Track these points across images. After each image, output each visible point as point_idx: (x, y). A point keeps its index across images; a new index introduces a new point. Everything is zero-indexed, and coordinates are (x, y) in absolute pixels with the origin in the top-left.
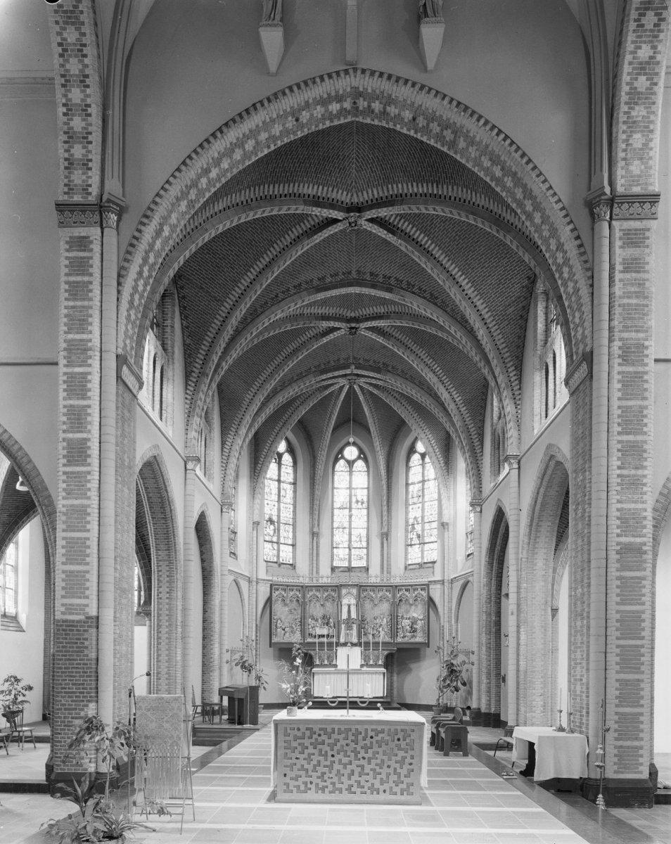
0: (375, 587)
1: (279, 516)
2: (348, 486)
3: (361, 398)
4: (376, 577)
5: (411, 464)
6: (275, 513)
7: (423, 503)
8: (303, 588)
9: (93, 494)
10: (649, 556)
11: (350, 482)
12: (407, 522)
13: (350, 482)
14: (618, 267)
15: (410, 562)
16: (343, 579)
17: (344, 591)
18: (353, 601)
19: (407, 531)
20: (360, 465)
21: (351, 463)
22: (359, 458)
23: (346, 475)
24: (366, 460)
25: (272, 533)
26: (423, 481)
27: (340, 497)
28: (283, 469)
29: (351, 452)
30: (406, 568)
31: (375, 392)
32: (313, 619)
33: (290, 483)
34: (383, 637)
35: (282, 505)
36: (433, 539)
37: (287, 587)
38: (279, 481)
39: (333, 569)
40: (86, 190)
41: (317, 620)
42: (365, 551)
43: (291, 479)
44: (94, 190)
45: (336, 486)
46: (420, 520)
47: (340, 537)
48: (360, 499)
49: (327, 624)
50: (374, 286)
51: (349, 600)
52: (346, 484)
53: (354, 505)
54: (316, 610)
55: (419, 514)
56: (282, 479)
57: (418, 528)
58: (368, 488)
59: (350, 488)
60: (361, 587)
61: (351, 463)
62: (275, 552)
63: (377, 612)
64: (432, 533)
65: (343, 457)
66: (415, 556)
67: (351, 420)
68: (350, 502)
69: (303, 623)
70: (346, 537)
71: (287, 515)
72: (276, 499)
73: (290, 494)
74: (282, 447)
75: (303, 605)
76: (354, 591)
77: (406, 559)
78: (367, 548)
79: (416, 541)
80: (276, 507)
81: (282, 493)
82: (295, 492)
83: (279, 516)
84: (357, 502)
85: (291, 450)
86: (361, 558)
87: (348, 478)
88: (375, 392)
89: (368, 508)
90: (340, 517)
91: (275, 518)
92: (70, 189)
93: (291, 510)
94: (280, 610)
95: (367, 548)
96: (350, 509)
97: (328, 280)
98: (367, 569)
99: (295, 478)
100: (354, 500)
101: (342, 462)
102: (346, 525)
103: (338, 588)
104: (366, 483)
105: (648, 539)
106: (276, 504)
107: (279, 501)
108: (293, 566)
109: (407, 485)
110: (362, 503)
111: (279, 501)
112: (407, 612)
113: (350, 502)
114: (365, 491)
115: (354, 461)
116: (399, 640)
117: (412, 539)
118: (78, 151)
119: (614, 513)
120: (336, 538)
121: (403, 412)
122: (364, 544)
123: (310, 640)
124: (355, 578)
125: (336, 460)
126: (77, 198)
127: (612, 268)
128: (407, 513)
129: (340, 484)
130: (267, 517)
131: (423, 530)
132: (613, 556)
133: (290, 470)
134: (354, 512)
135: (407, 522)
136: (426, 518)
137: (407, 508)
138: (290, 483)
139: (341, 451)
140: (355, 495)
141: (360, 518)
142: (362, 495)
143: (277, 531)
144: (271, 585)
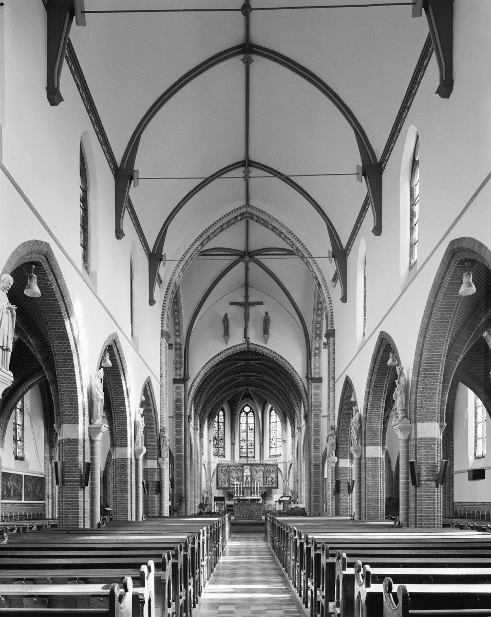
0: (257, 465)
1: (218, 436)
3: (251, 393)
4: (258, 461)
5: (271, 414)
7: (276, 431)
8: (228, 466)
9: (183, 452)
10: (321, 466)
11: (247, 421)
12: (270, 438)
13: (247, 421)
14: (313, 395)
15: (271, 455)
16: (244, 461)
17: (245, 467)
18: (249, 471)
19: (270, 442)
20: (251, 414)
21: (247, 413)
22: (250, 411)
23: (245, 418)
24: (253, 412)
26: (276, 422)
27: (243, 427)
29: (247, 409)
30: (270, 457)
31: (257, 392)
32: (233, 478)
34: (260, 484)
37: (223, 466)
38: (218, 422)
39: (240, 457)
40: (180, 375)
41: (234, 479)
44: (182, 375)
46: (275, 437)
49: (238, 480)
50: (254, 372)
51: (247, 472)
52: (245, 422)
54: (234, 475)
55: (275, 435)
57: (274, 440)
58: (254, 424)
59: (247, 424)
60: (251, 465)
61: (247, 413)
63: (258, 475)
64: (279, 443)
65: (244, 411)
66: (273, 452)
67: (247, 396)
68: (247, 429)
69: (229, 480)
70: (245, 444)
75: (228, 472)
76: (249, 467)
77: (270, 453)
78: (254, 448)
79: (274, 446)
81: (219, 427)
82: (224, 426)
83: (218, 436)
84: (250, 429)
87: (246, 419)
88: (257, 392)
89: (254, 432)
91: (217, 437)
92: (176, 375)
94: (221, 476)
96: (247, 432)
97: (239, 371)
98: (254, 457)
99: (224, 421)
100: (248, 428)
101: (243, 413)
102: (245, 439)
103: (242, 465)
105: (321, 462)
108: (224, 456)
110: (252, 430)
112: (270, 475)
113: (247, 429)
116: (267, 486)
118: (178, 366)
119: (312, 456)
120: (242, 444)
121: (267, 399)
122: (253, 447)
123: (231, 486)
124: (251, 461)
125: (241, 412)
126: (178, 377)
127: (311, 394)
128: (270, 435)
131: (276, 442)
132: (312, 466)
133: (222, 417)
135: (270, 438)
137: (270, 432)
139: (243, 408)
142: (252, 426)
144: (217, 465)
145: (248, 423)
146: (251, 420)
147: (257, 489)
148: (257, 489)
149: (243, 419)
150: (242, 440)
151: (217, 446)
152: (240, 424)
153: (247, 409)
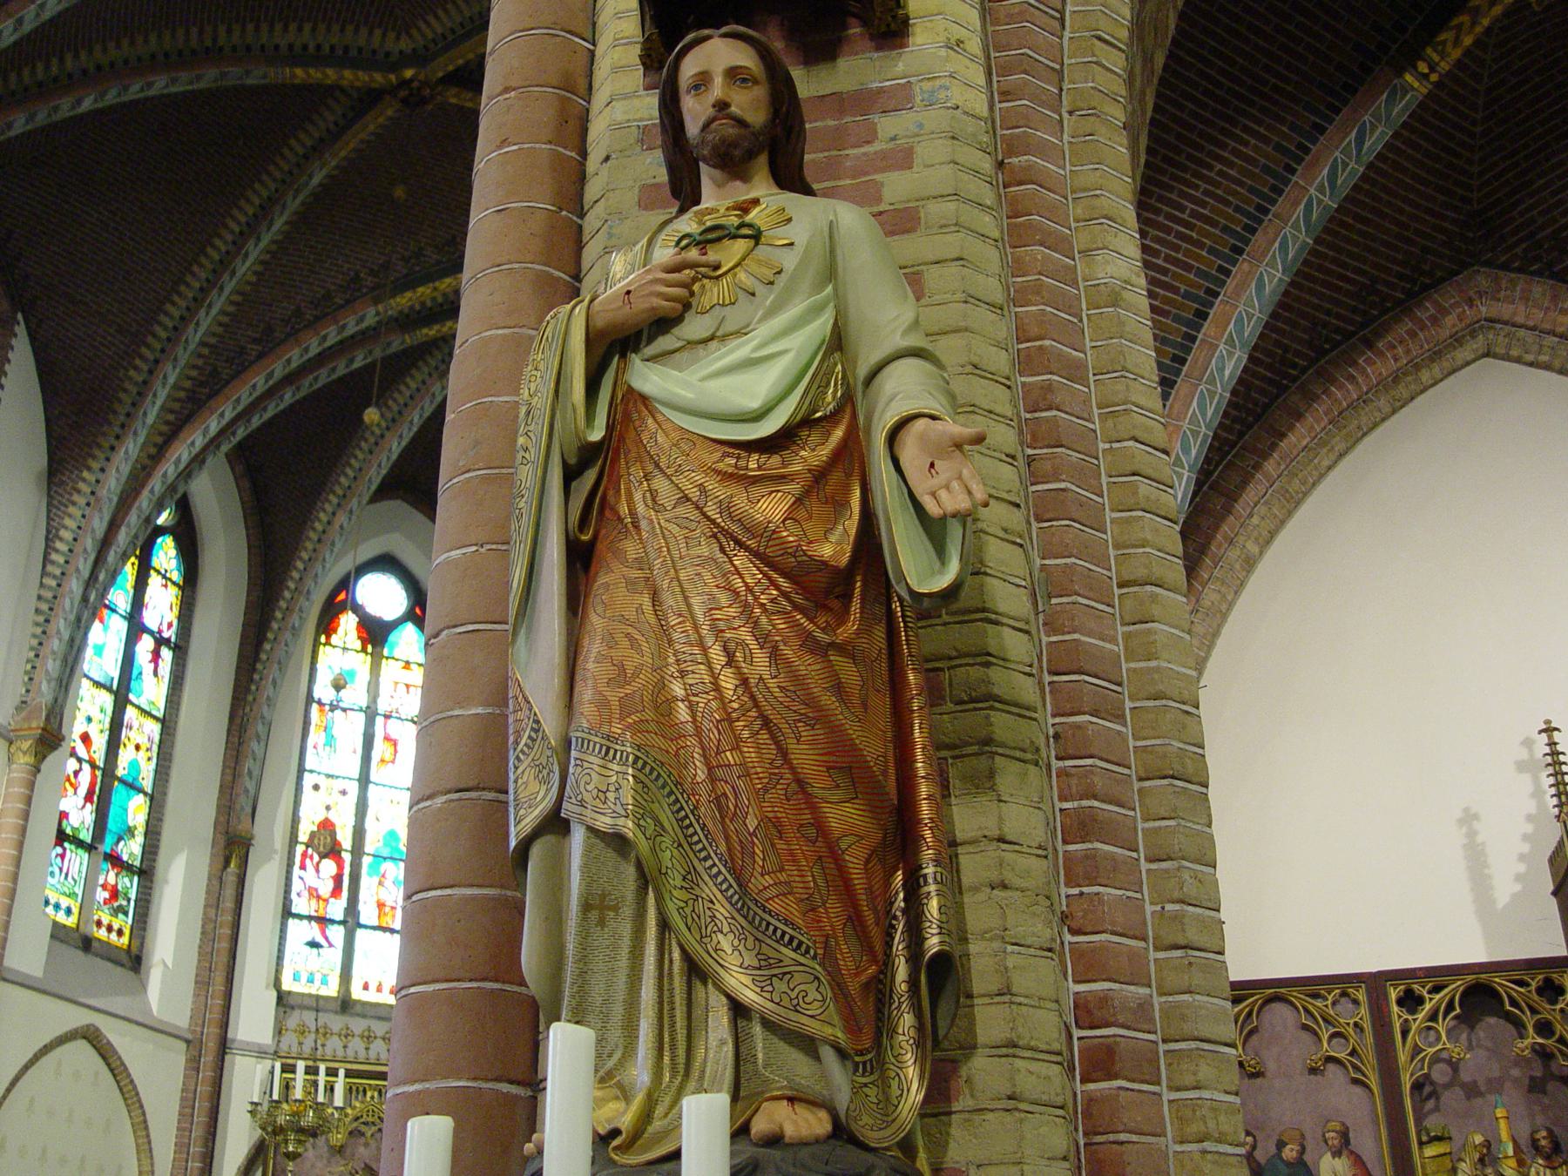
1: (359, 834)
25: (326, 888)
28: (389, 670)
81: (380, 749)
83: (359, 834)
91: (345, 838)
106: (353, 789)
107: (364, 780)
111: (364, 780)
143: (349, 885)
151: (337, 909)
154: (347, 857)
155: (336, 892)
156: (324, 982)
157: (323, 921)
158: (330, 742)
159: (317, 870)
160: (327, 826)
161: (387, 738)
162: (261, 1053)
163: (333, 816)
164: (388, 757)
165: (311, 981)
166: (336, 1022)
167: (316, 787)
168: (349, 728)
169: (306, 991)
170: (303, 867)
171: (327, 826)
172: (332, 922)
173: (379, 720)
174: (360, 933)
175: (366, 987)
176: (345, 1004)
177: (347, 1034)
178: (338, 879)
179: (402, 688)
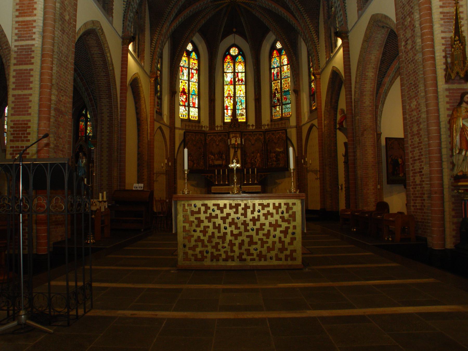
2: (233, 71)
6: (186, 88)
7: (281, 79)
21: (234, 58)
23: (232, 65)
27: (229, 77)
28: (192, 61)
33: (196, 70)
35: (190, 83)
36: (288, 101)
38: (189, 68)
42: (245, 110)
43: (196, 67)
45: (225, 71)
46: (279, 90)
47: (228, 103)
48: (240, 79)
52: (230, 70)
53: (237, 83)
56: (191, 67)
57: (278, 95)
58: (245, 72)
62: (187, 112)
71: (194, 87)
72: (187, 79)
73: (196, 77)
74: (190, 47)
80: (187, 84)
84: (239, 80)
85: (195, 49)
86: (242, 115)
89: (246, 85)
90: (228, 89)
91: (186, 91)
93: (197, 86)
95: (246, 109)
99: (199, 66)
100: (237, 79)
104: (244, 68)
106: (187, 82)
107: (189, 81)
109: (270, 69)
111: (189, 81)
114: (244, 74)
115: (236, 56)
117: (274, 102)
122: (244, 106)
129: (227, 69)
130: (181, 90)
134: (237, 87)
136: (283, 88)
138: (196, 70)
140: (238, 76)
141: (240, 91)
142: (241, 76)
143: (188, 99)
145: (237, 71)
146: (240, 68)
147: (253, 172)
148: (253, 172)
149: (228, 68)
150: (227, 97)
151: (187, 104)
152: (224, 72)
153: (234, 51)
154: (187, 94)
155: (186, 101)
156: (186, 117)
157: (185, 106)
158: (183, 74)
159: (183, 97)
160: (184, 89)
161: (192, 73)
162: (180, 129)
163: (185, 87)
164: (192, 76)
165: (184, 116)
166: (188, 123)
167: (182, 82)
168: (185, 72)
169: (183, 118)
170: (181, 97)
171: (184, 89)
172: (186, 106)
173: (190, 70)
174: (191, 108)
175: (192, 117)
176: (189, 120)
177: (189, 126)
178: (186, 98)
179: (193, 64)
